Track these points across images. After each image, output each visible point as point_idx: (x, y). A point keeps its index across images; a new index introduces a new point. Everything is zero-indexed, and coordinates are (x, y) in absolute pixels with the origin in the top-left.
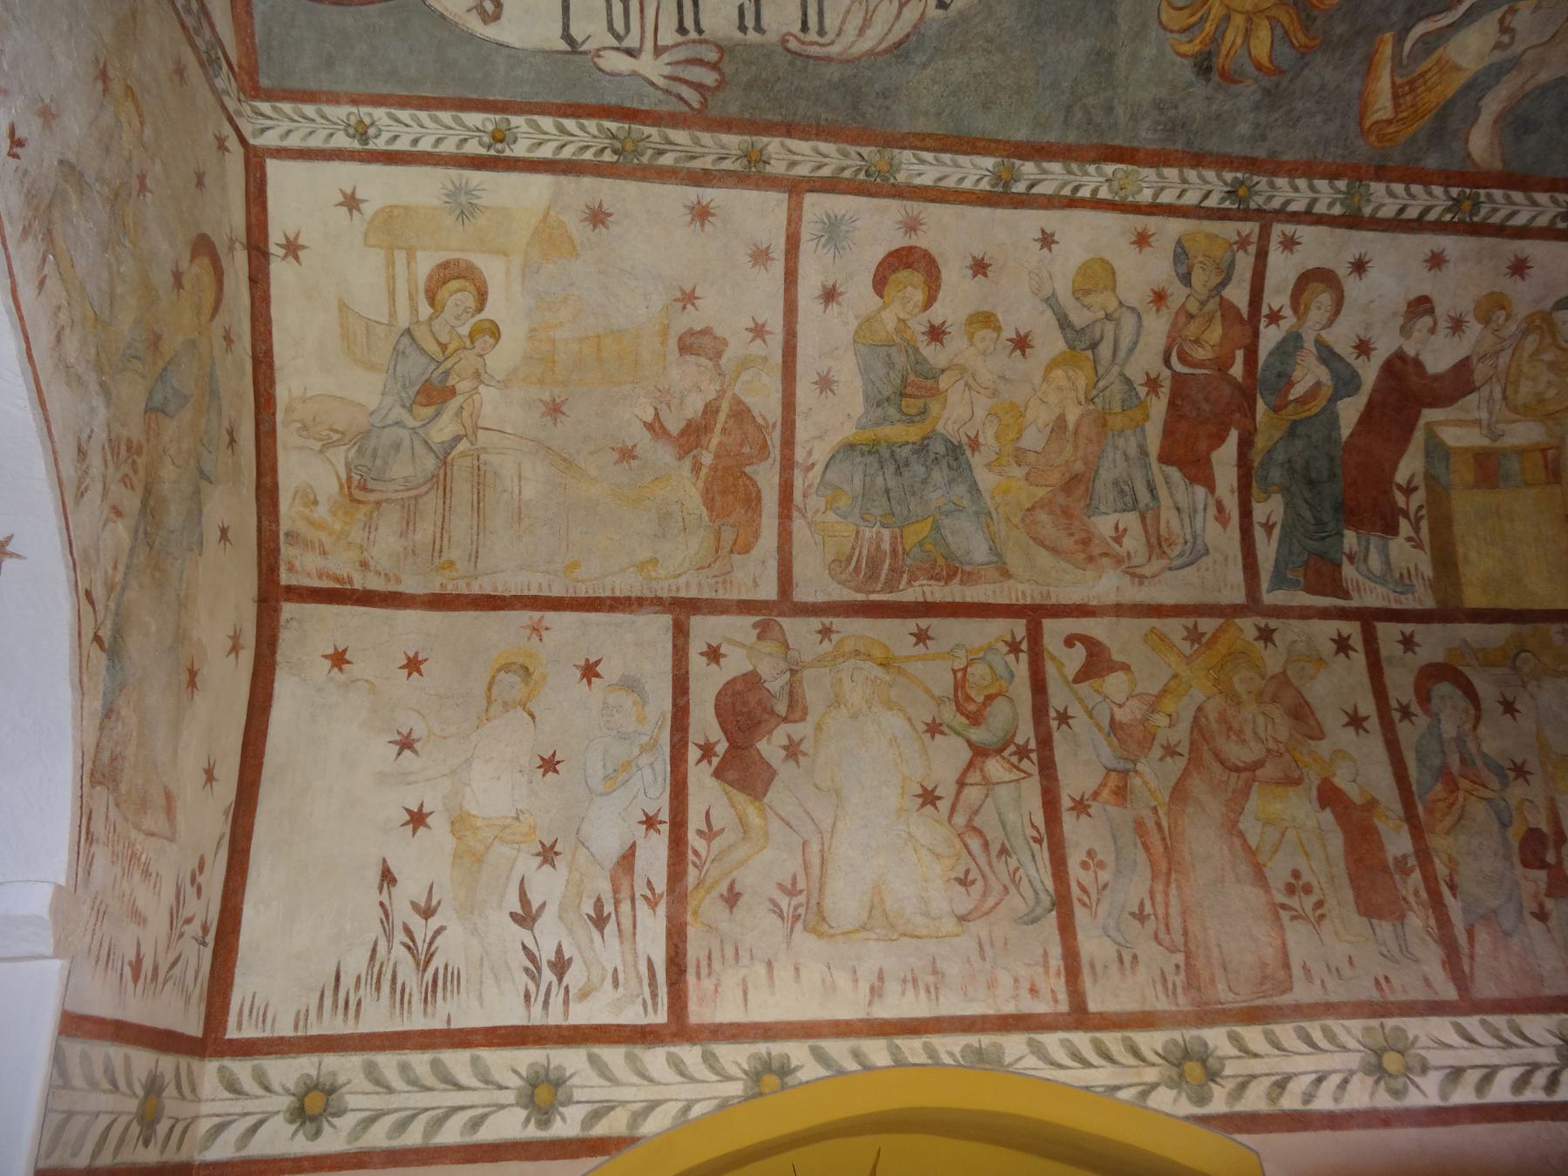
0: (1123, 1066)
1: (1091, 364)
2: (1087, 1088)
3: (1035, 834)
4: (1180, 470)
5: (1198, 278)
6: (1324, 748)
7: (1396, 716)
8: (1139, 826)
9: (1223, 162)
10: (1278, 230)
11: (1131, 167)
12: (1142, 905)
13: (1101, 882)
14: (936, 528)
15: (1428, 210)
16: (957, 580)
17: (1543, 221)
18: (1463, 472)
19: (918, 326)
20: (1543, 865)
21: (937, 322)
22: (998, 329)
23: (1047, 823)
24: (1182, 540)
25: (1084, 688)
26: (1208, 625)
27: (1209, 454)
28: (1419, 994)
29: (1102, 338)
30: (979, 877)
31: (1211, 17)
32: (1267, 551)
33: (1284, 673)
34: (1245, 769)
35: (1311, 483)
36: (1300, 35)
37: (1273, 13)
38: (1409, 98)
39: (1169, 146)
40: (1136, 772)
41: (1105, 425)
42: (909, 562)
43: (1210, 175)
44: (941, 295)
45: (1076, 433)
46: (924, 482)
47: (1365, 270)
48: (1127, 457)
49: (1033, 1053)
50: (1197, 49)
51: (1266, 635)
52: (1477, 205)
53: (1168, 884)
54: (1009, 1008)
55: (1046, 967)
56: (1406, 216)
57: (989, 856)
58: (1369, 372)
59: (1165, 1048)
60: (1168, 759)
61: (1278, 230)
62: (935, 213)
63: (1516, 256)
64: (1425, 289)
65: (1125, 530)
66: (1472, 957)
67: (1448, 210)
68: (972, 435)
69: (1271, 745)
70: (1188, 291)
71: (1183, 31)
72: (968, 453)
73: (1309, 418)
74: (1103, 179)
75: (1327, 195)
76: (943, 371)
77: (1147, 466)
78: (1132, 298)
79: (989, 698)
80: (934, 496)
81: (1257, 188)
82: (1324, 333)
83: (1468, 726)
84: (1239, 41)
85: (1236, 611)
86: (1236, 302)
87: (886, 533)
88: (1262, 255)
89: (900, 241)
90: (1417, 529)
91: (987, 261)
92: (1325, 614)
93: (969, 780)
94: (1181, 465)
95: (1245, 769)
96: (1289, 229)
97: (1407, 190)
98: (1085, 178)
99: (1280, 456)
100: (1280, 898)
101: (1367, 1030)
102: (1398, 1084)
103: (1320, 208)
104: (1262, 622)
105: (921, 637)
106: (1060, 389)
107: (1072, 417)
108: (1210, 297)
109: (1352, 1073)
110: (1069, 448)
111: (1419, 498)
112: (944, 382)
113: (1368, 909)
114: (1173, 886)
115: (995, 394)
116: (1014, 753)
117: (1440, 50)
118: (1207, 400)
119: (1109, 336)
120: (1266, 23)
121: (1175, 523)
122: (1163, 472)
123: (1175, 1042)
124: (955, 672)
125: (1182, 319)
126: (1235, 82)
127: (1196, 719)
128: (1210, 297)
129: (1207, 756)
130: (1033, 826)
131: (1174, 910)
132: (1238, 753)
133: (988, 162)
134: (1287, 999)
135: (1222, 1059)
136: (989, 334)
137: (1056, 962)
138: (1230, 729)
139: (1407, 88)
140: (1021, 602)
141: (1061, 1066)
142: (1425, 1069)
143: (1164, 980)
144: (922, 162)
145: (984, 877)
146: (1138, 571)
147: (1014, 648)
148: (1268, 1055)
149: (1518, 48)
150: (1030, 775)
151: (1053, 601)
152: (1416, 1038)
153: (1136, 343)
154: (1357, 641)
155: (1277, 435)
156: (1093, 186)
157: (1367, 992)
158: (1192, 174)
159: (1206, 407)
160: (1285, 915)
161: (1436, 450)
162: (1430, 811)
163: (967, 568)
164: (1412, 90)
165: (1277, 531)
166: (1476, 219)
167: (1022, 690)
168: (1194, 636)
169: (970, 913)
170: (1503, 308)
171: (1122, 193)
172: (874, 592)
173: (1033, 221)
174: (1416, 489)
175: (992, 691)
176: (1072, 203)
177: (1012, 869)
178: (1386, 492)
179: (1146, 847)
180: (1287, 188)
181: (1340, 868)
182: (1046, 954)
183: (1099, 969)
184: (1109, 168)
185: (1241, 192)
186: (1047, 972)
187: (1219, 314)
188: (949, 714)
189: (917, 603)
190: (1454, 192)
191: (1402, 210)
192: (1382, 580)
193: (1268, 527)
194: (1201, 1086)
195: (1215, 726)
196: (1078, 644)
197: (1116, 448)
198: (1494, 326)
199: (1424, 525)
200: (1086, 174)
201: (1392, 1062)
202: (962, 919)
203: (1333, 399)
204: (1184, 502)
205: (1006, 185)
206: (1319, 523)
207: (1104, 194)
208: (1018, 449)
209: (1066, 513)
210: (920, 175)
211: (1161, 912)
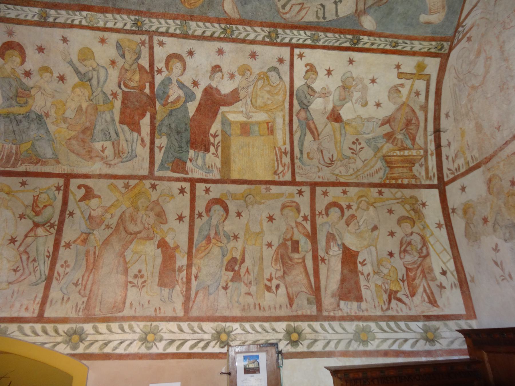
0: (50, 336)
1: (89, 87)
2: (34, 343)
3: (48, 255)
4: (128, 126)
5: (127, 55)
6: (165, 227)
7: (196, 216)
8: (87, 253)
9: (129, 12)
10: (156, 39)
11: (93, 13)
12: (78, 280)
13: (66, 272)
14: (33, 145)
15: (214, 33)
16: (40, 164)
17: (260, 38)
18: (236, 130)
19: (20, 71)
20: (233, 270)
21: (28, 70)
22: (52, 73)
23: (53, 251)
24: (127, 152)
25: (82, 204)
26: (132, 182)
27: (139, 121)
28: (170, 313)
29: (92, 77)
30: (22, 269)
32: (159, 157)
33: (158, 200)
34: (134, 234)
35: (178, 133)
39: (106, 6)
40: (93, 234)
41: (97, 109)
42: (22, 157)
43: (125, 17)
44: (27, 60)
45: (86, 112)
46: (28, 128)
47: (193, 55)
48: (106, 122)
49: (18, 330)
51: (154, 187)
52: (232, 31)
53: (91, 273)
54: (15, 315)
55: (34, 301)
56: (205, 35)
57: (28, 262)
58: (199, 93)
59: (68, 330)
60: (107, 230)
61: (156, 39)
62: (18, 29)
63: (251, 51)
64: (218, 63)
65: (106, 148)
66: (194, 302)
67: (222, 33)
68: (46, 112)
69: (146, 226)
70: (123, 61)
72: (45, 118)
73: (177, 109)
74: (83, 17)
75: (173, 26)
76: (32, 88)
77: (114, 125)
78: (102, 62)
79: (45, 206)
80: (32, 134)
81: (145, 22)
82: (179, 78)
83: (222, 220)
85: (144, 178)
86: (143, 65)
87: (14, 147)
88: (151, 48)
89: (7, 39)
90: (217, 151)
91: (43, 47)
92: (178, 180)
93: (30, 235)
94: (128, 125)
95: (134, 234)
96: (161, 38)
97: (204, 25)
98: (75, 17)
99: (166, 123)
100: (130, 279)
101: (145, 326)
102: (149, 345)
103: (171, 31)
104: (153, 182)
105: (23, 184)
106: (79, 96)
107: (84, 105)
108: (133, 63)
109: (134, 340)
110: (84, 118)
111: (219, 139)
112: (33, 92)
113: (162, 284)
114: (92, 274)
115: (53, 97)
116: (49, 226)
118: (137, 101)
119: (95, 76)
121: (125, 145)
122: (121, 127)
123: (72, 328)
124: (34, 196)
125: (123, 71)
127: (121, 216)
128: (133, 63)
129: (121, 228)
130: (48, 252)
131: (89, 283)
132: (132, 228)
133: (36, 10)
134: (120, 314)
135: (87, 335)
136: (48, 74)
137: (39, 300)
138: (133, 219)
140: (63, 172)
141: (27, 335)
142: (161, 340)
143: (77, 306)
144: (9, 9)
145: (24, 269)
146: (109, 162)
147: (58, 189)
148: (105, 334)
150: (52, 234)
151: (75, 172)
152: (162, 329)
153: (106, 79)
154: (188, 190)
155: (165, 115)
156: (79, 20)
157: (151, 312)
158: (118, 16)
159: (136, 103)
160: (130, 285)
161: (225, 122)
162: (197, 250)
163: (44, 160)
165: (163, 150)
166: (233, 37)
167: (58, 204)
168: (127, 186)
169: (14, 281)
170: (248, 70)
171: (92, 23)
172: (7, 167)
173: (58, 32)
174: (218, 136)
175: (47, 204)
176: (72, 26)
177: (35, 266)
178: (206, 137)
179: (87, 260)
180: (157, 23)
181: (157, 270)
182: (36, 297)
183: (53, 302)
184: (84, 13)
185: (139, 24)
186: (34, 303)
187: (138, 69)
188: (29, 212)
189: (23, 172)
190: (223, 26)
191: (204, 32)
192: (201, 168)
193: (160, 148)
194: (76, 344)
195: (127, 218)
196: (83, 188)
197: (102, 118)
198: (245, 77)
199: (220, 149)
200: (76, 15)
201: (150, 337)
202: (10, 283)
203: (185, 102)
204: (129, 137)
205: (45, 19)
206: (180, 147)
207: (84, 23)
208: (64, 117)
209: (83, 141)
210: (9, 14)
211: (84, 283)
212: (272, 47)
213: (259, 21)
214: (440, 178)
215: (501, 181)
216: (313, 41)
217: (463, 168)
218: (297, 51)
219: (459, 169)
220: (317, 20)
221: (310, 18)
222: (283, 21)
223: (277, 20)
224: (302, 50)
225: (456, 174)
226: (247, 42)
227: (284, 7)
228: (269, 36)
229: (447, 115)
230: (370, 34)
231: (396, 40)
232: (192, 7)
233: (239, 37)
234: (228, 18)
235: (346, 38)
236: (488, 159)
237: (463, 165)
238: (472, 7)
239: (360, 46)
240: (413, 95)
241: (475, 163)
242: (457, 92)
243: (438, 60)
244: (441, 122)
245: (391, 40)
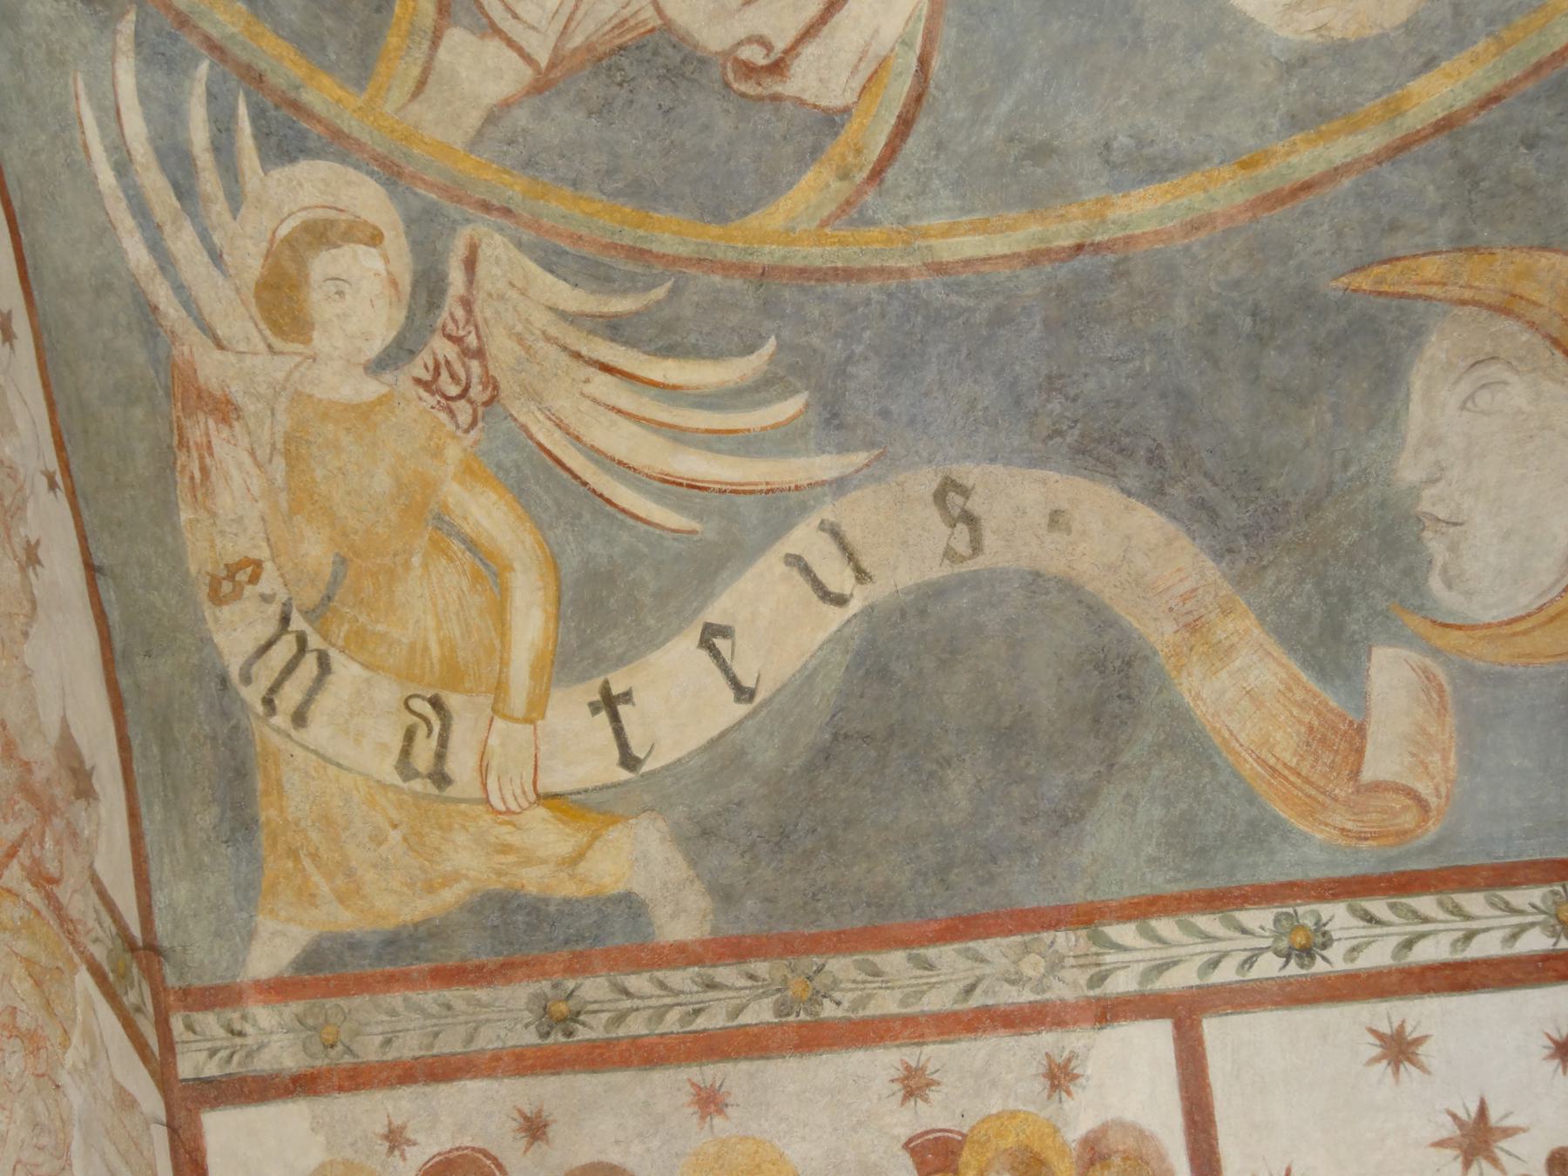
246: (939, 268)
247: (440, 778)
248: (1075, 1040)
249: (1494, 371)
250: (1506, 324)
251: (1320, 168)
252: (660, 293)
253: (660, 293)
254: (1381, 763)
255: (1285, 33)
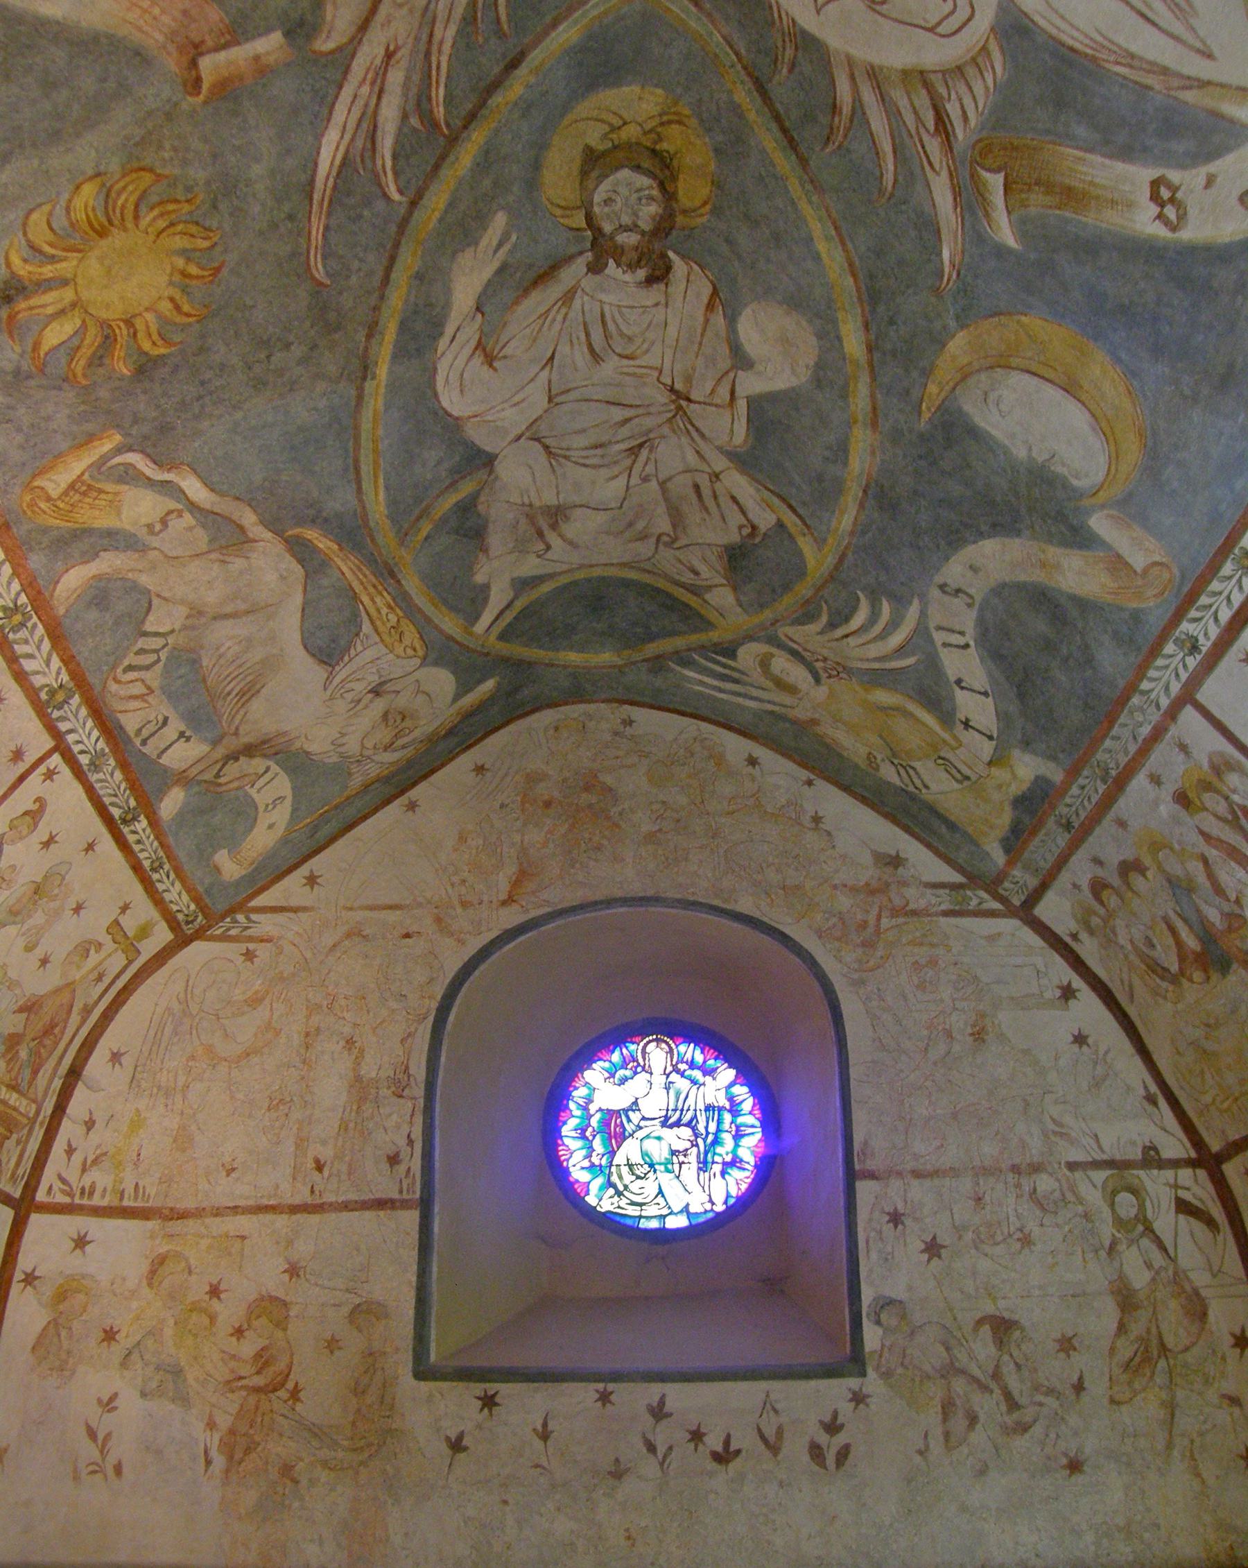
17: (38, 681)
31: (58, 266)
36: (82, 363)
37: (89, 322)
38: (77, 497)
50: (22, 273)
52: (23, 625)
71: (32, 247)
84: (50, 310)
117: (126, 487)
120: (78, 322)
126: (12, 337)
139: (84, 488)
149: (155, 542)
164: (84, 494)
166: (11, 636)
190: (23, 599)
212: (33, 714)
213: (74, 651)
214: (31, 1187)
215: (190, 1273)
216: (92, 763)
217: (103, 1196)
218: (56, 759)
219: (91, 1194)
220: (132, 734)
221: (130, 723)
222: (98, 688)
223: (94, 680)
224: (66, 771)
225: (77, 1201)
226: (15, 666)
227: (130, 668)
228: (52, 693)
229: (116, 1057)
230: (154, 823)
231: (165, 860)
232: (29, 513)
233: (16, 647)
234: (47, 594)
235: (127, 802)
236: (183, 1215)
237: (105, 1190)
238: (285, 904)
239: (126, 830)
240: (96, 974)
241: (139, 1204)
242: (168, 1030)
243: (170, 936)
244: (92, 1060)
245: (161, 853)
246: (852, 533)
247: (967, 778)
248: (1173, 731)
249: (992, 396)
250: (972, 381)
251: (868, 400)
252: (825, 607)
253: (825, 607)
254: (1138, 561)
255: (804, 379)
